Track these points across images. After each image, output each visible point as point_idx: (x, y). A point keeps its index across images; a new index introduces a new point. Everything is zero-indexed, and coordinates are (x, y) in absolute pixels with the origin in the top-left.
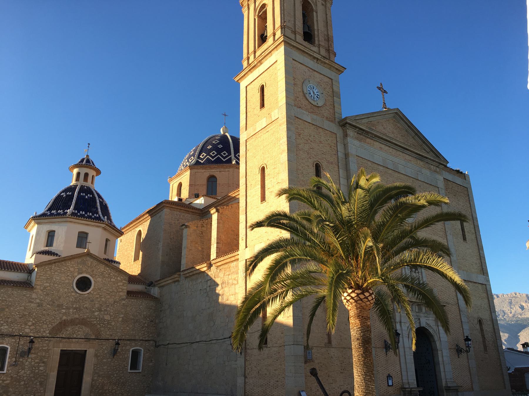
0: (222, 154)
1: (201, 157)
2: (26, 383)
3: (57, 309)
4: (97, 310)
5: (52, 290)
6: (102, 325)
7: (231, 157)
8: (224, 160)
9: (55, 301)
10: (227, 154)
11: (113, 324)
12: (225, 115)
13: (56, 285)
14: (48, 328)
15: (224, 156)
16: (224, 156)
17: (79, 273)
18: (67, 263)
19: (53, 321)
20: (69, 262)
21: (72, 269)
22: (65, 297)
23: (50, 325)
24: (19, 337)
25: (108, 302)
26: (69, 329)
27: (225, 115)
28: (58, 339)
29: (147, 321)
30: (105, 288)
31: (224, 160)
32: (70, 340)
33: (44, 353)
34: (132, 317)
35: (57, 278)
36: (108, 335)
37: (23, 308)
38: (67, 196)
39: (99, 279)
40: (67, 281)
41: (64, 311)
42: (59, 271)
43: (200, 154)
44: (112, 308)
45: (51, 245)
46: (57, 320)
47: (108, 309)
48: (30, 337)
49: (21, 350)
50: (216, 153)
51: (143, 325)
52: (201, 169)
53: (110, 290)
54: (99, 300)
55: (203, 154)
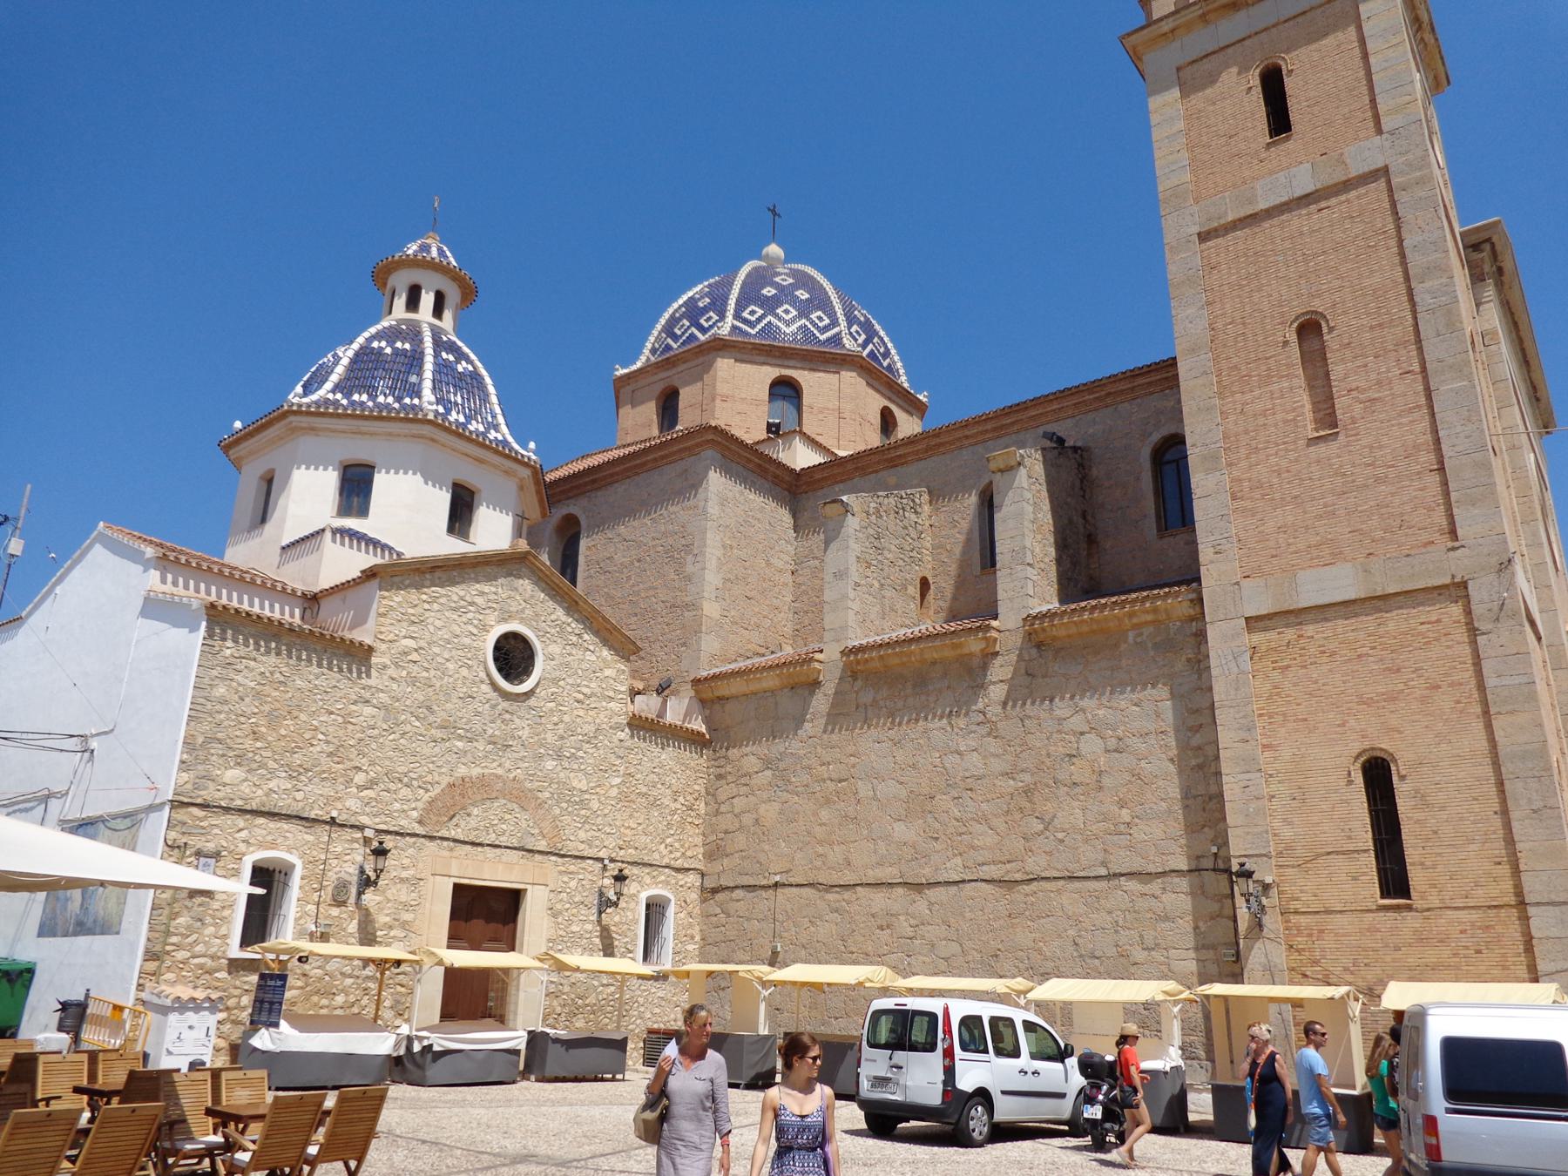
1: (745, 315)
2: (352, 998)
3: (441, 735)
4: (551, 752)
5: (425, 665)
6: (564, 805)
8: (822, 338)
9: (435, 708)
10: (827, 321)
11: (595, 805)
12: (774, 212)
13: (436, 650)
14: (417, 800)
15: (821, 325)
17: (504, 620)
18: (466, 576)
19: (429, 778)
20: (473, 576)
21: (480, 600)
22: (462, 695)
23: (421, 791)
24: (327, 827)
25: (579, 730)
26: (475, 811)
27: (774, 212)
28: (445, 843)
29: (680, 806)
30: (570, 681)
32: (480, 849)
33: (404, 890)
34: (644, 790)
35: (438, 623)
36: (582, 842)
37: (340, 720)
38: (396, 352)
39: (555, 649)
40: (467, 641)
41: (460, 744)
42: (442, 600)
44: (591, 751)
45: (363, 512)
46: (440, 774)
47: (580, 754)
48: (361, 828)
49: (335, 876)
51: (669, 818)
52: (754, 352)
53: (585, 690)
54: (556, 719)
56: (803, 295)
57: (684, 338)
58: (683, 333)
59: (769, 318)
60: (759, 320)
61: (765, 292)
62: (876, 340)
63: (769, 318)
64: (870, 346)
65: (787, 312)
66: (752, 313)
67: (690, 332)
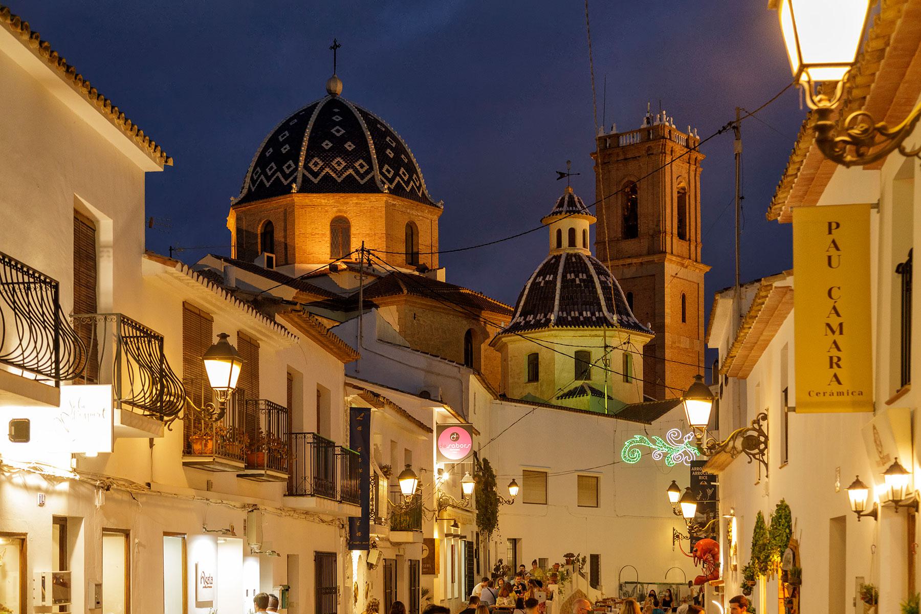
0: (357, 165)
1: (311, 165)
7: (373, 177)
8: (362, 182)
10: (367, 167)
16: (362, 171)
31: (362, 182)
43: (308, 158)
50: (344, 164)
55: (316, 159)
56: (349, 146)
57: (273, 179)
58: (273, 174)
59: (327, 170)
60: (322, 169)
61: (324, 145)
62: (402, 170)
63: (327, 170)
64: (398, 179)
65: (339, 164)
66: (316, 164)
67: (276, 175)
